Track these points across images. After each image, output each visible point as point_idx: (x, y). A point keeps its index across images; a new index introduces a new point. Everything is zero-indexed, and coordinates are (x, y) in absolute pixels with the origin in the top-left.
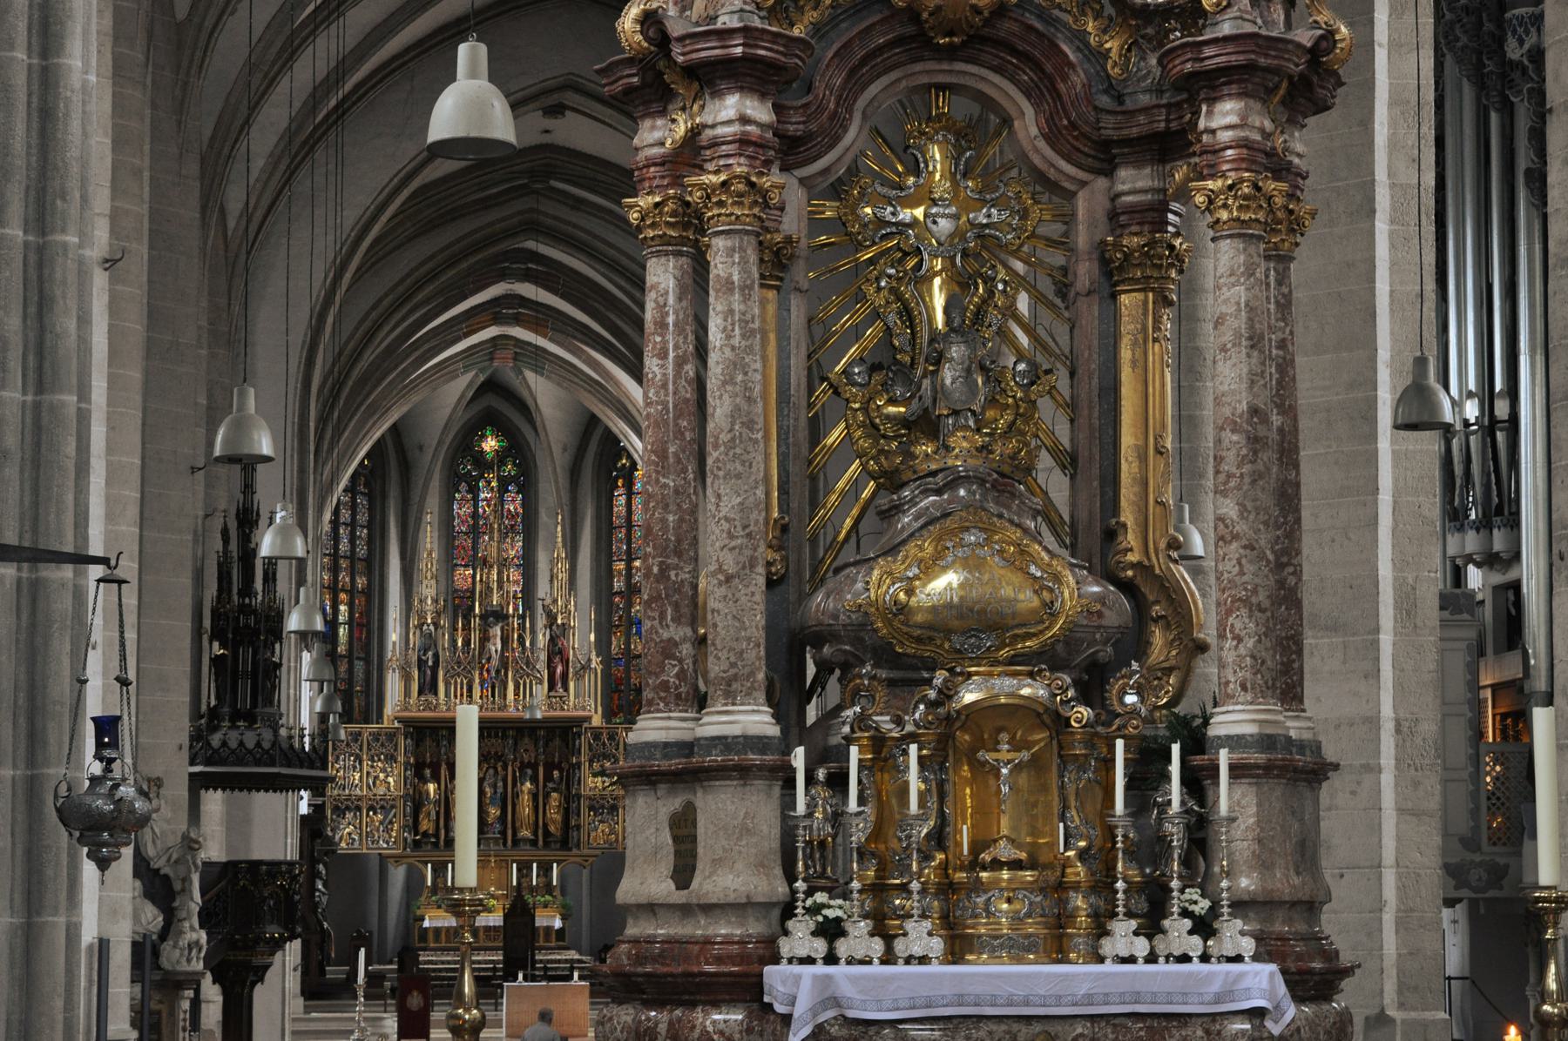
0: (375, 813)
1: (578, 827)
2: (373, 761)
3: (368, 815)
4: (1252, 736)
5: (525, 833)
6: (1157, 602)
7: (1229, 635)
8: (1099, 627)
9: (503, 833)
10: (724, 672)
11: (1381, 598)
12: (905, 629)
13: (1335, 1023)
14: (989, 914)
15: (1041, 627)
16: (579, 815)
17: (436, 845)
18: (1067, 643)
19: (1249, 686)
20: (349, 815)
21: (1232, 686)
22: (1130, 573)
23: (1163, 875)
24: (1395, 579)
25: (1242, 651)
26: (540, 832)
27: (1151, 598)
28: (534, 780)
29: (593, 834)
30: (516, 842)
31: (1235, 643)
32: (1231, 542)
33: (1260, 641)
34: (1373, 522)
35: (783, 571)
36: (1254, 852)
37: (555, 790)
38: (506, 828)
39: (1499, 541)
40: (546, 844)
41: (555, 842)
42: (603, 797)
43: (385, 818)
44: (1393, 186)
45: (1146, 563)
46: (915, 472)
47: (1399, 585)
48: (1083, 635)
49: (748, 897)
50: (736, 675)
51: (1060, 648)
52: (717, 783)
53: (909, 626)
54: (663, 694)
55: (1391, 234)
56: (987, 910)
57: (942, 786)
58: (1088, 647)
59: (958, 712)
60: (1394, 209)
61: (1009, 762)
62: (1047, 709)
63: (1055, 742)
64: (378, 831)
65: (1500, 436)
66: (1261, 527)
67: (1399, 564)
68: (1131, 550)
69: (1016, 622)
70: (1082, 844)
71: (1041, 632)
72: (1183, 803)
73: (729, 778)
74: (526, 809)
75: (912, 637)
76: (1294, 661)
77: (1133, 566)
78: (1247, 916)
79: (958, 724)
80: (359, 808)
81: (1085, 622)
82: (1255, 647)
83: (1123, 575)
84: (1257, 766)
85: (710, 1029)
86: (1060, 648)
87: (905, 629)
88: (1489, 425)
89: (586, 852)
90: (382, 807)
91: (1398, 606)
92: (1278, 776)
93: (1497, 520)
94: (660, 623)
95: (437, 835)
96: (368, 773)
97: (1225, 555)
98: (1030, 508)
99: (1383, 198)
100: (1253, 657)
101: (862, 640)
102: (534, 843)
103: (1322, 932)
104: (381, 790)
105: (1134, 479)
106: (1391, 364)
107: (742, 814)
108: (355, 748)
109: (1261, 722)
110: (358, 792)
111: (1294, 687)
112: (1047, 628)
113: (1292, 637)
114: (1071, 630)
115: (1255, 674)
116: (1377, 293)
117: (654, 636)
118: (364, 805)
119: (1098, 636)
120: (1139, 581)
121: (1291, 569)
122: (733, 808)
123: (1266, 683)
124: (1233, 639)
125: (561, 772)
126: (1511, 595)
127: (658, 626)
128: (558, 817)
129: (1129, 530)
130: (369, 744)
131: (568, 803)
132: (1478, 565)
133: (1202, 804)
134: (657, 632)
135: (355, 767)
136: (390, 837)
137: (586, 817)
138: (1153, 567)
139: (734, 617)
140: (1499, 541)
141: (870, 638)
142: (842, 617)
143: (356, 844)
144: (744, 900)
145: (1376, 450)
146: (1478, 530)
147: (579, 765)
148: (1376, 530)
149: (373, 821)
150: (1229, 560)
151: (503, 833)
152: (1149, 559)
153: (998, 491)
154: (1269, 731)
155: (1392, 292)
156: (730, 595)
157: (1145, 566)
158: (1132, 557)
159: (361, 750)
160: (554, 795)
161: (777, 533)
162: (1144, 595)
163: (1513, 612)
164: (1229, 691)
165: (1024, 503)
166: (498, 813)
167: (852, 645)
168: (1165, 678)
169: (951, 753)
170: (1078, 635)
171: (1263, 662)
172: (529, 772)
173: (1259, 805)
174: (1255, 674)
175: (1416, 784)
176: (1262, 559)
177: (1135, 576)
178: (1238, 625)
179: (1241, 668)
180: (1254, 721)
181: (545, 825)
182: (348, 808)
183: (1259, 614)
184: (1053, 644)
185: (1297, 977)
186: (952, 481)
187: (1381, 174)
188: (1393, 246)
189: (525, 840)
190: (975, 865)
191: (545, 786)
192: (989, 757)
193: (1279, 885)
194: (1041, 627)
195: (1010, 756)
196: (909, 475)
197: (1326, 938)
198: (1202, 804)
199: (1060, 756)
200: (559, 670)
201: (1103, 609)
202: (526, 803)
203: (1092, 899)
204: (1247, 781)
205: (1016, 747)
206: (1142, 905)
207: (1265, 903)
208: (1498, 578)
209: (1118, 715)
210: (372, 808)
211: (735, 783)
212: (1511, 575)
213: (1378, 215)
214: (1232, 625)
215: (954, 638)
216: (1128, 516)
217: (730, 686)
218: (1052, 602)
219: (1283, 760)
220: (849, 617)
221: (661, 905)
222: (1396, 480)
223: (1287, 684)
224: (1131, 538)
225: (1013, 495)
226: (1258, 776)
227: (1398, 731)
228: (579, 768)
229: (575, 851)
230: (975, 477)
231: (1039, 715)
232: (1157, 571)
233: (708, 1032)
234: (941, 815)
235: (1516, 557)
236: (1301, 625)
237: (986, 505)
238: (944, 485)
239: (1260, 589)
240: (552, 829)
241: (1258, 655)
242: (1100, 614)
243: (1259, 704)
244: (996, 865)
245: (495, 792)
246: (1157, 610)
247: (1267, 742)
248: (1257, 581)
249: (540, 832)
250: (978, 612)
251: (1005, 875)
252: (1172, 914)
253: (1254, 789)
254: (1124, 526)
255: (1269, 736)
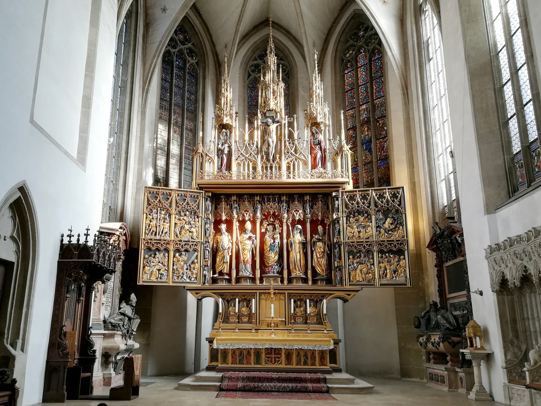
0: (180, 255)
1: (340, 268)
2: (181, 216)
3: (174, 256)
5: (297, 273)
9: (281, 273)
16: (340, 258)
17: (229, 281)
20: (159, 255)
26: (309, 272)
28: (303, 232)
29: (353, 273)
30: (290, 281)
37: (319, 240)
38: (283, 269)
40: (314, 282)
41: (322, 280)
42: (360, 243)
43: (189, 259)
64: (182, 268)
74: (296, 254)
80: (167, 250)
89: (348, 287)
90: (186, 251)
95: (230, 274)
96: (176, 224)
102: (305, 281)
104: (186, 236)
108: (166, 204)
110: (167, 238)
118: (171, 248)
125: (324, 226)
128: (323, 261)
130: (177, 203)
131: (330, 250)
135: (165, 219)
136: (192, 274)
137: (346, 261)
143: (164, 279)
147: (337, 220)
149: (178, 261)
151: (281, 273)
159: (171, 206)
160: (320, 244)
166: (277, 258)
172: (300, 227)
181: (313, 268)
182: (158, 250)
189: (297, 278)
191: (312, 237)
200: (319, 155)
202: (297, 250)
210: (178, 250)
228: (338, 222)
229: (339, 287)
240: (319, 270)
245: (274, 242)
249: (309, 272)
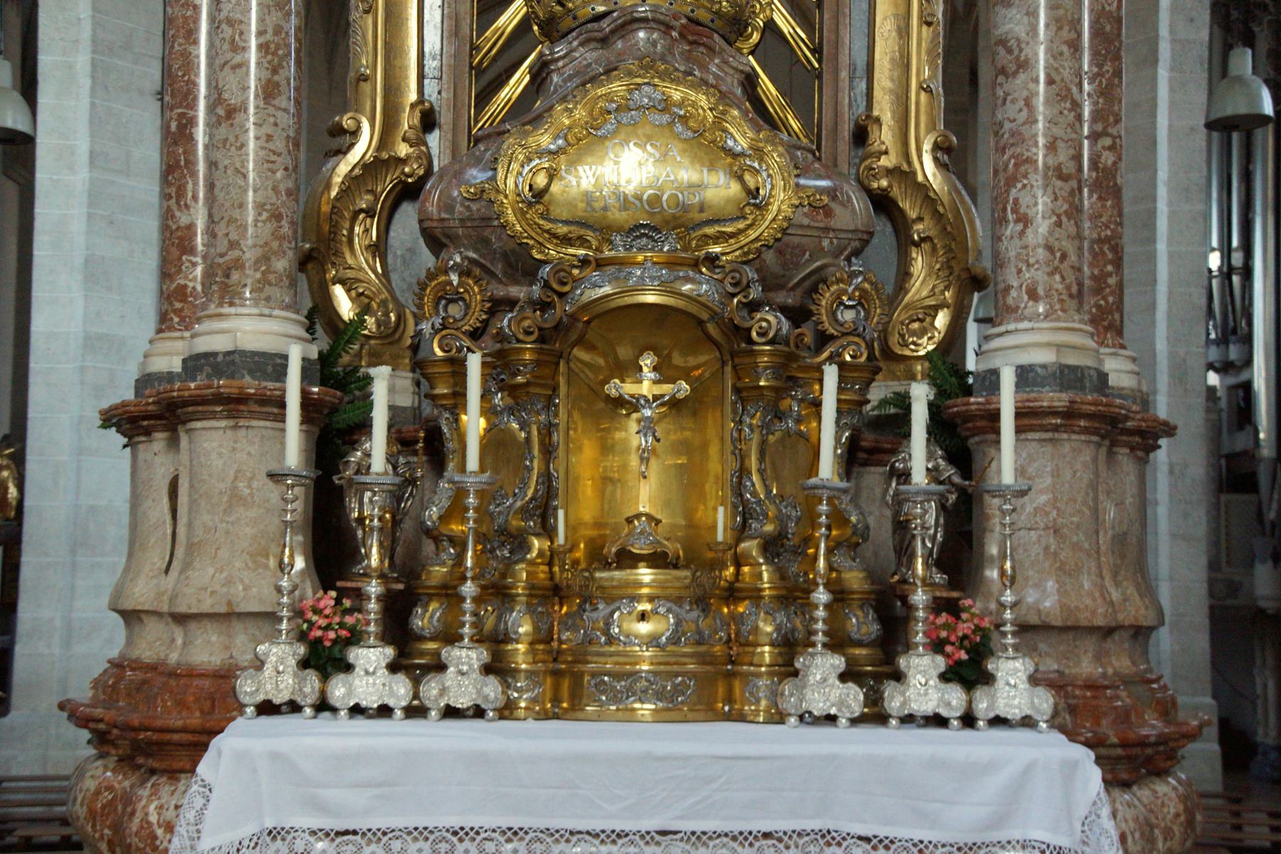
4: (1044, 366)
6: (920, 219)
7: (1010, 216)
8: (827, 229)
10: (222, 256)
11: (1158, 367)
12: (548, 226)
13: (1177, 815)
14: (611, 640)
15: (741, 225)
18: (780, 252)
19: (1041, 291)
21: (1014, 293)
22: (884, 183)
23: (904, 581)
24: (1170, 353)
25: (1030, 238)
27: (913, 214)
31: (1020, 227)
32: (1015, 73)
33: (1059, 224)
34: (1153, 307)
35: (421, 172)
36: (1047, 548)
39: (1234, 353)
44: (1173, 41)
45: (905, 167)
46: (575, 18)
47: (1172, 355)
48: (804, 240)
49: (229, 603)
50: (238, 260)
51: (769, 256)
52: (198, 424)
53: (550, 220)
54: (178, 305)
55: (1171, 80)
56: (606, 632)
57: (550, 435)
58: (812, 260)
59: (573, 317)
60: (1173, 59)
61: (656, 398)
62: (714, 315)
63: (728, 369)
65: (1236, 279)
66: (1065, 48)
67: (1173, 340)
68: (886, 153)
69: (704, 216)
70: (769, 528)
71: (740, 232)
72: (933, 473)
73: (213, 416)
75: (555, 236)
76: (1110, 275)
77: (889, 172)
78: (1035, 649)
79: (573, 337)
81: (806, 221)
82: (1051, 233)
83: (875, 185)
84: (1054, 413)
85: (153, 818)
86: (769, 256)
87: (548, 226)
88: (1227, 272)
91: (1172, 375)
92: (1086, 431)
93: (1232, 338)
94: (178, 203)
97: (1007, 94)
98: (736, 69)
99: (1165, 50)
100: (1049, 248)
101: (486, 242)
103: (1150, 670)
105: (892, 60)
106: (1169, 182)
107: (232, 473)
109: (1059, 347)
111: (1110, 312)
112: (749, 226)
113: (1107, 240)
114: (784, 231)
115: (1051, 274)
116: (1158, 125)
117: (170, 223)
119: (826, 243)
120: (896, 192)
121: (1107, 142)
122: (220, 463)
123: (1068, 288)
124: (1017, 221)
126: (1241, 393)
127: (174, 207)
129: (884, 128)
132: (1217, 371)
133: (966, 472)
134: (173, 216)
138: (914, 173)
139: (237, 171)
140: (1234, 353)
141: (499, 238)
142: (458, 208)
144: (223, 609)
145: (1155, 251)
146: (1218, 345)
148: (1154, 314)
150: (1013, 102)
152: (910, 163)
153: (691, 43)
154: (1072, 360)
155: (1170, 126)
156: (232, 139)
157: (903, 173)
158: (884, 162)
161: (416, 121)
162: (902, 212)
163: (1242, 404)
164: (1010, 301)
165: (726, 62)
167: (476, 250)
168: (928, 319)
169: (562, 381)
170: (796, 240)
171: (1064, 257)
173: (1056, 474)
174: (1051, 274)
175: (1186, 515)
176: (1064, 99)
177: (890, 186)
178: (1025, 200)
179: (1029, 265)
180: (1049, 345)
183: (1059, 183)
184: (759, 251)
185: (1119, 751)
186: (623, 25)
187: (1164, 31)
188: (1172, 90)
190: (598, 557)
192: (629, 388)
193: (1088, 601)
194: (741, 225)
195: (658, 390)
196: (568, 23)
197: (1158, 680)
198: (966, 472)
199: (737, 390)
201: (833, 205)
203: (781, 617)
204: (1037, 435)
205: (665, 372)
206: (861, 624)
207: (1065, 629)
208: (1232, 380)
209: (832, 338)
211: (223, 423)
212: (1243, 377)
213: (1161, 64)
214: (1016, 201)
215: (618, 239)
216: (884, 108)
217: (228, 276)
218: (758, 189)
219: (1095, 404)
220: (468, 208)
221: (147, 612)
222: (1171, 274)
223: (1098, 307)
224: (885, 136)
225: (711, 49)
226: (1056, 429)
227: (1171, 472)
230: (654, 20)
231: (701, 323)
232: (920, 178)
233: (149, 823)
234: (547, 477)
235: (1248, 362)
236: (1121, 224)
237: (669, 58)
238: (613, 32)
239: (1060, 144)
241: (1056, 244)
242: (828, 212)
243: (1058, 320)
244: (627, 559)
246: (919, 230)
247: (1068, 376)
248: (1057, 131)
250: (649, 202)
251: (645, 574)
252: (917, 645)
253: (1049, 448)
254: (878, 121)
255: (1073, 369)
